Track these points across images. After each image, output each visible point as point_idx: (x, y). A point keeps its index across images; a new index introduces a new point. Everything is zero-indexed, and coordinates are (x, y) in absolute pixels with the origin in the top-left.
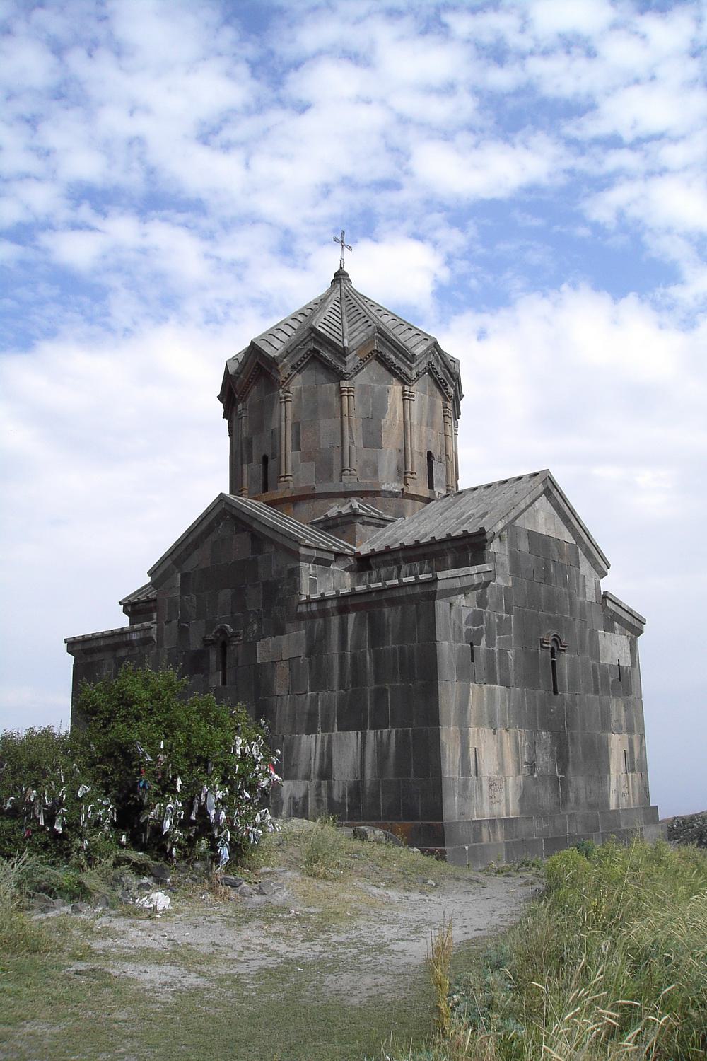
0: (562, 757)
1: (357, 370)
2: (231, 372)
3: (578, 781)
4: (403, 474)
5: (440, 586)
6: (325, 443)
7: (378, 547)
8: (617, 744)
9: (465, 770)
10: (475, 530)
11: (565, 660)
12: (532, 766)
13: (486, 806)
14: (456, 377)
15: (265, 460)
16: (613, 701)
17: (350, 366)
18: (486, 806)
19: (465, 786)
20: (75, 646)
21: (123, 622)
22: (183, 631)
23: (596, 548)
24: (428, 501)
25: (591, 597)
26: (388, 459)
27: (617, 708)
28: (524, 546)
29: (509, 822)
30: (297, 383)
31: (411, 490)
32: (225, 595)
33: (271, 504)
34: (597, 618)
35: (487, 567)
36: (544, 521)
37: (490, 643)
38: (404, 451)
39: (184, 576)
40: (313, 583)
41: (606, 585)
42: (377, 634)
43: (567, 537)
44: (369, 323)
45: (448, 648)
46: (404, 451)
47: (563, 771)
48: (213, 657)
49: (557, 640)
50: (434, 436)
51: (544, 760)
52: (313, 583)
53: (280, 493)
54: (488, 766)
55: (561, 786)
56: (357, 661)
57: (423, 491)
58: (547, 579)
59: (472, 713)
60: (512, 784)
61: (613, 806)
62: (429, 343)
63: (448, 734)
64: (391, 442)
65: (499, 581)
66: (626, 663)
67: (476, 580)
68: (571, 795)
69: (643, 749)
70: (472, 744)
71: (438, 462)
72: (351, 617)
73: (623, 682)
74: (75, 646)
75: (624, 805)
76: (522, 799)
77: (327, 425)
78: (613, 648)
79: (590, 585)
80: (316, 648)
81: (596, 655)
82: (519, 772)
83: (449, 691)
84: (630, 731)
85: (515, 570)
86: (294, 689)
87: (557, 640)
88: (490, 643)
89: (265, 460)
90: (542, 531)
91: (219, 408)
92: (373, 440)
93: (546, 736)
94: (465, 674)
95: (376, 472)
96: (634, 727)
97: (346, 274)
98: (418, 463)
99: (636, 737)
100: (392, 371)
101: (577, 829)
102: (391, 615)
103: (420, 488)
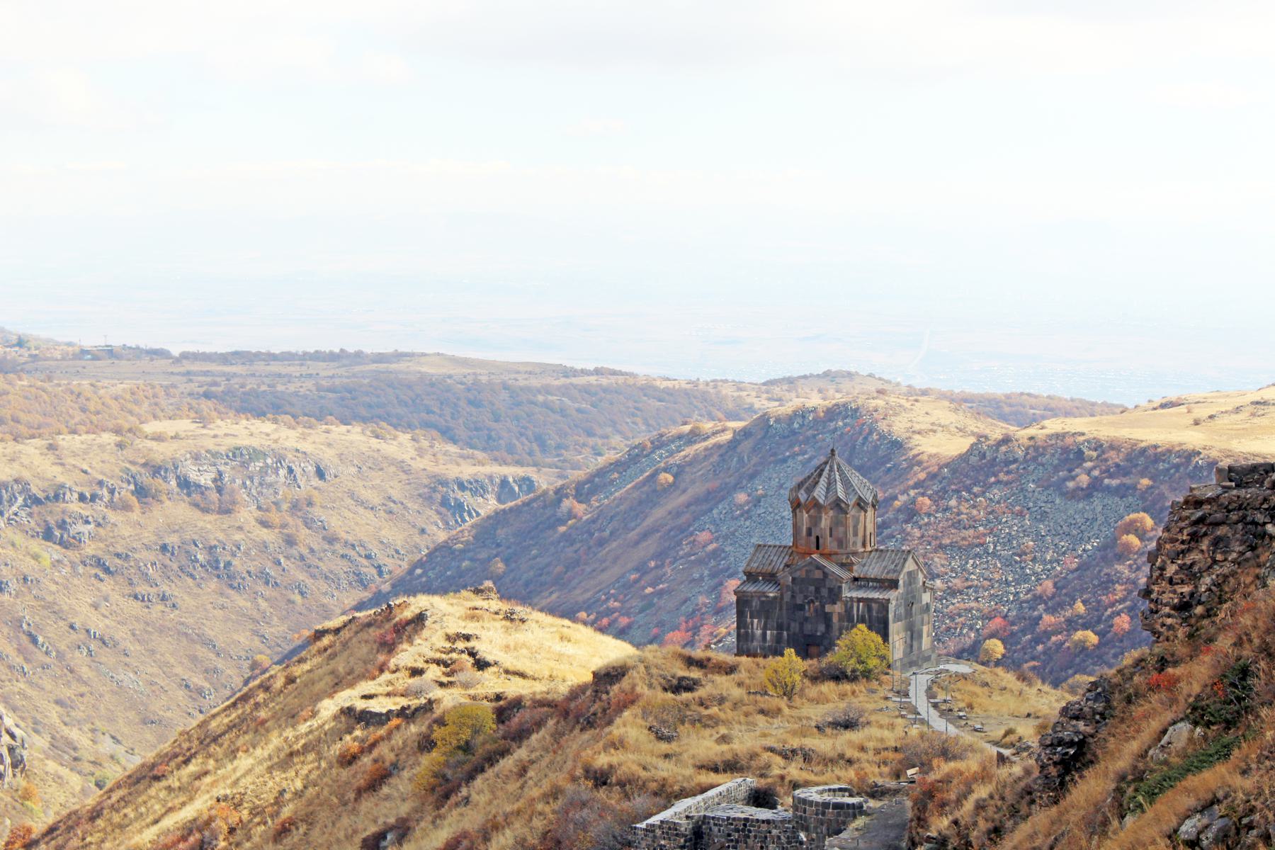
2: (802, 500)
3: (915, 644)
4: (864, 545)
6: (841, 535)
8: (925, 629)
15: (818, 538)
22: (793, 597)
27: (926, 617)
30: (831, 513)
32: (812, 588)
33: (822, 555)
38: (865, 536)
39: (794, 579)
42: (870, 609)
45: (891, 616)
46: (865, 536)
53: (826, 551)
55: (911, 646)
56: (863, 617)
57: (869, 549)
77: (841, 529)
80: (848, 612)
86: (840, 620)
89: (818, 538)
92: (856, 534)
94: (894, 622)
100: (862, 508)
102: (874, 606)
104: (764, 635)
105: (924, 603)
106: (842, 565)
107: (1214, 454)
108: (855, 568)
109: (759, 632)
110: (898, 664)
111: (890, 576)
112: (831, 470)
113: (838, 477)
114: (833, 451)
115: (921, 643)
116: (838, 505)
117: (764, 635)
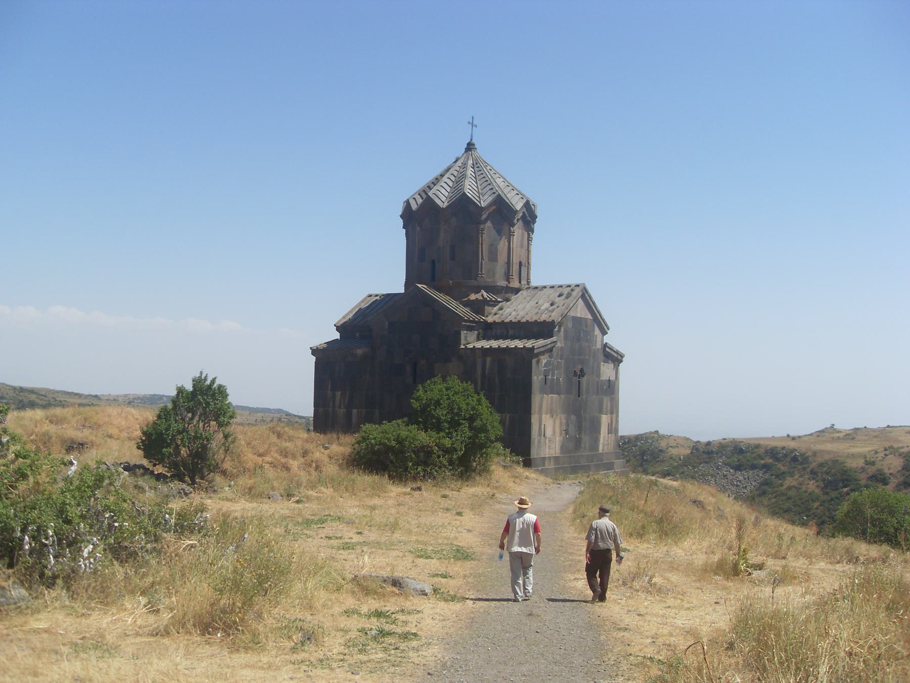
0: (580, 428)
1: (487, 220)
2: (414, 207)
3: (586, 439)
5: (536, 351)
7: (497, 319)
8: (605, 419)
9: (540, 435)
10: (550, 320)
11: (584, 380)
12: (567, 432)
13: (547, 450)
14: (534, 217)
15: (433, 262)
16: (605, 398)
17: (484, 217)
18: (547, 450)
19: (539, 441)
20: (315, 351)
21: (337, 336)
23: (604, 320)
24: (517, 291)
25: (599, 346)
26: (500, 269)
28: (570, 325)
29: (556, 459)
31: (511, 285)
34: (601, 356)
35: (554, 339)
36: (581, 311)
37: (553, 376)
40: (466, 337)
41: (607, 339)
43: (590, 317)
44: (494, 191)
45: (537, 379)
46: (509, 263)
47: (580, 434)
48: (409, 369)
49: (582, 370)
50: (524, 251)
51: (572, 429)
52: (466, 337)
54: (549, 433)
55: (578, 443)
58: (579, 340)
59: (544, 408)
60: (558, 439)
61: (600, 451)
62: (525, 201)
63: (534, 419)
64: (502, 258)
65: (559, 344)
66: (613, 378)
67: (549, 346)
68: (583, 445)
69: (617, 422)
70: (543, 423)
71: (525, 265)
72: (488, 359)
73: (611, 388)
74: (315, 351)
75: (606, 451)
76: (562, 447)
78: (607, 371)
79: (599, 339)
81: (599, 376)
82: (561, 435)
83: (536, 398)
84: (612, 413)
85: (566, 338)
87: (582, 370)
88: (553, 376)
89: (433, 262)
90: (579, 315)
91: (401, 222)
92: (493, 257)
93: (573, 417)
94: (543, 391)
95: (494, 274)
96: (614, 410)
97: (474, 145)
98: (515, 268)
99: (614, 416)
101: (583, 462)
103: (515, 284)
104: (349, 415)
105: (604, 377)
106: (468, 304)
107: (803, 450)
108: (488, 309)
109: (342, 411)
110: (550, 466)
111: (544, 317)
112: (464, 166)
113: (470, 171)
114: (470, 147)
115: (596, 440)
116: (462, 203)
117: (349, 415)
